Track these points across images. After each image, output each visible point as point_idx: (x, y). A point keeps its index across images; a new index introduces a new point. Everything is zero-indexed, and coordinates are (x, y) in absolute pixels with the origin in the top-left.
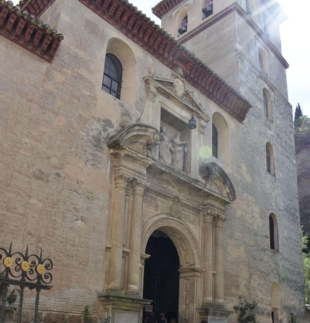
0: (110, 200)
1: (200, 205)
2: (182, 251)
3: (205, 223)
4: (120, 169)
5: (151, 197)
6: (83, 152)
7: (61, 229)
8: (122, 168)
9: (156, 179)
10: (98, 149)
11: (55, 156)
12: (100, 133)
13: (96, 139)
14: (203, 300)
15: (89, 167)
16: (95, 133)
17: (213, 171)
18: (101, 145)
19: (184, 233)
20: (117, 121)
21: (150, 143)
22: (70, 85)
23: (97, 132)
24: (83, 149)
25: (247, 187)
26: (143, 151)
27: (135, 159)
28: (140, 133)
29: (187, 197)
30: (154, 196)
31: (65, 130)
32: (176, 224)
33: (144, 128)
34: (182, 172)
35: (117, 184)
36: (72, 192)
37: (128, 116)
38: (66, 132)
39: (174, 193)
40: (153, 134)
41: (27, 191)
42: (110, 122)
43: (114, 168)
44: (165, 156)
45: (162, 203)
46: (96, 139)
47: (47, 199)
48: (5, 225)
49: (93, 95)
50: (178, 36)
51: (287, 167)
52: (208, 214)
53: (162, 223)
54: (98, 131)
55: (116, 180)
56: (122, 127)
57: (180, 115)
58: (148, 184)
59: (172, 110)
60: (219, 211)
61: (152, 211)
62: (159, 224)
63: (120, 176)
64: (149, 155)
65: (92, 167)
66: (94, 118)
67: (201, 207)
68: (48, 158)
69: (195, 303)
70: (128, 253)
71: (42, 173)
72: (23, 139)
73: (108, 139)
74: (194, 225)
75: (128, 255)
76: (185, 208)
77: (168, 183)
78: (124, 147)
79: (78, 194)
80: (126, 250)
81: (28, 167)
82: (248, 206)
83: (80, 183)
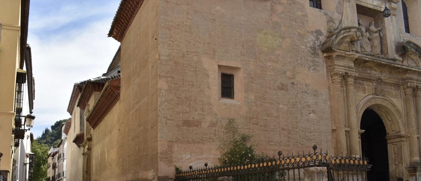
0: (330, 93)
1: (400, 80)
2: (388, 122)
3: (405, 95)
4: (334, 68)
5: (359, 83)
6: (306, 62)
7: (301, 122)
8: (336, 67)
9: (361, 67)
10: (315, 56)
11: (288, 70)
12: (315, 43)
13: (312, 49)
14: (411, 160)
15: (311, 72)
16: (311, 44)
17: (408, 49)
18: (317, 52)
19: (389, 107)
20: (325, 28)
21: (354, 40)
22: (288, 12)
23: (313, 43)
24: (305, 59)
26: (349, 48)
27: (344, 57)
28: (345, 35)
29: (388, 76)
30: (361, 82)
31: (291, 48)
32: (382, 101)
33: (348, 30)
34: (381, 56)
35: (333, 80)
36: (304, 94)
37: (332, 21)
38: (292, 49)
39: (377, 76)
40: (355, 33)
41: (276, 100)
42: (320, 31)
44: (367, 48)
45: (369, 86)
46: (312, 49)
47: (289, 102)
48: (268, 126)
49: (305, 14)
52: (408, 87)
53: (369, 103)
54: (313, 42)
55: (332, 77)
56: (330, 32)
57: (373, 5)
58: (357, 75)
59: (366, 3)
61: (362, 94)
62: (368, 104)
63: (336, 74)
64: (353, 49)
65: (313, 71)
66: (308, 32)
67: (401, 82)
68: (285, 72)
69: (404, 163)
70: (348, 131)
71: (283, 85)
72: (267, 64)
73: (321, 46)
74: (396, 98)
75: (348, 133)
76: (387, 86)
77: (371, 68)
78: (335, 50)
79: (308, 94)
80: (347, 129)
81: (274, 83)
83: (308, 86)
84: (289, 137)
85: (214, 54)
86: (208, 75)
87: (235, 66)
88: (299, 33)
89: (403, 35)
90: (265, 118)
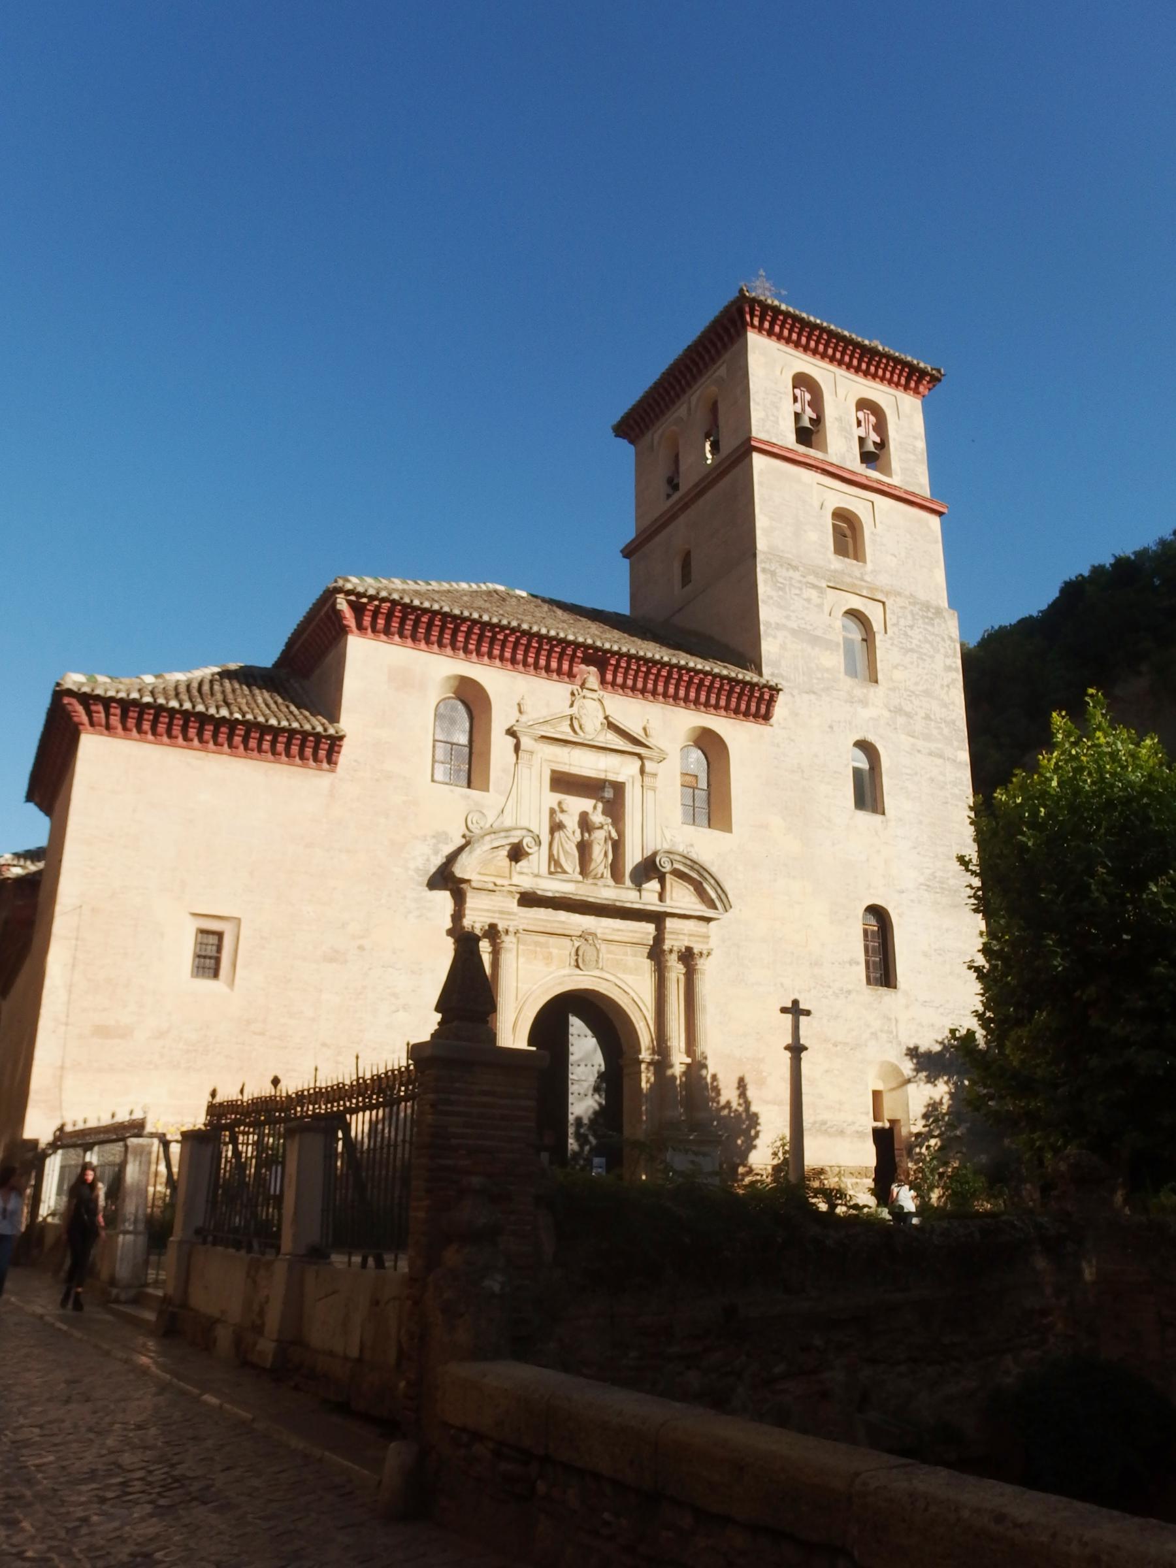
12: (428, 860)
30: (542, 939)
33: (503, 834)
42: (446, 833)
50: (669, 496)
51: (932, 780)
60: (692, 938)
84: (337, 1062)
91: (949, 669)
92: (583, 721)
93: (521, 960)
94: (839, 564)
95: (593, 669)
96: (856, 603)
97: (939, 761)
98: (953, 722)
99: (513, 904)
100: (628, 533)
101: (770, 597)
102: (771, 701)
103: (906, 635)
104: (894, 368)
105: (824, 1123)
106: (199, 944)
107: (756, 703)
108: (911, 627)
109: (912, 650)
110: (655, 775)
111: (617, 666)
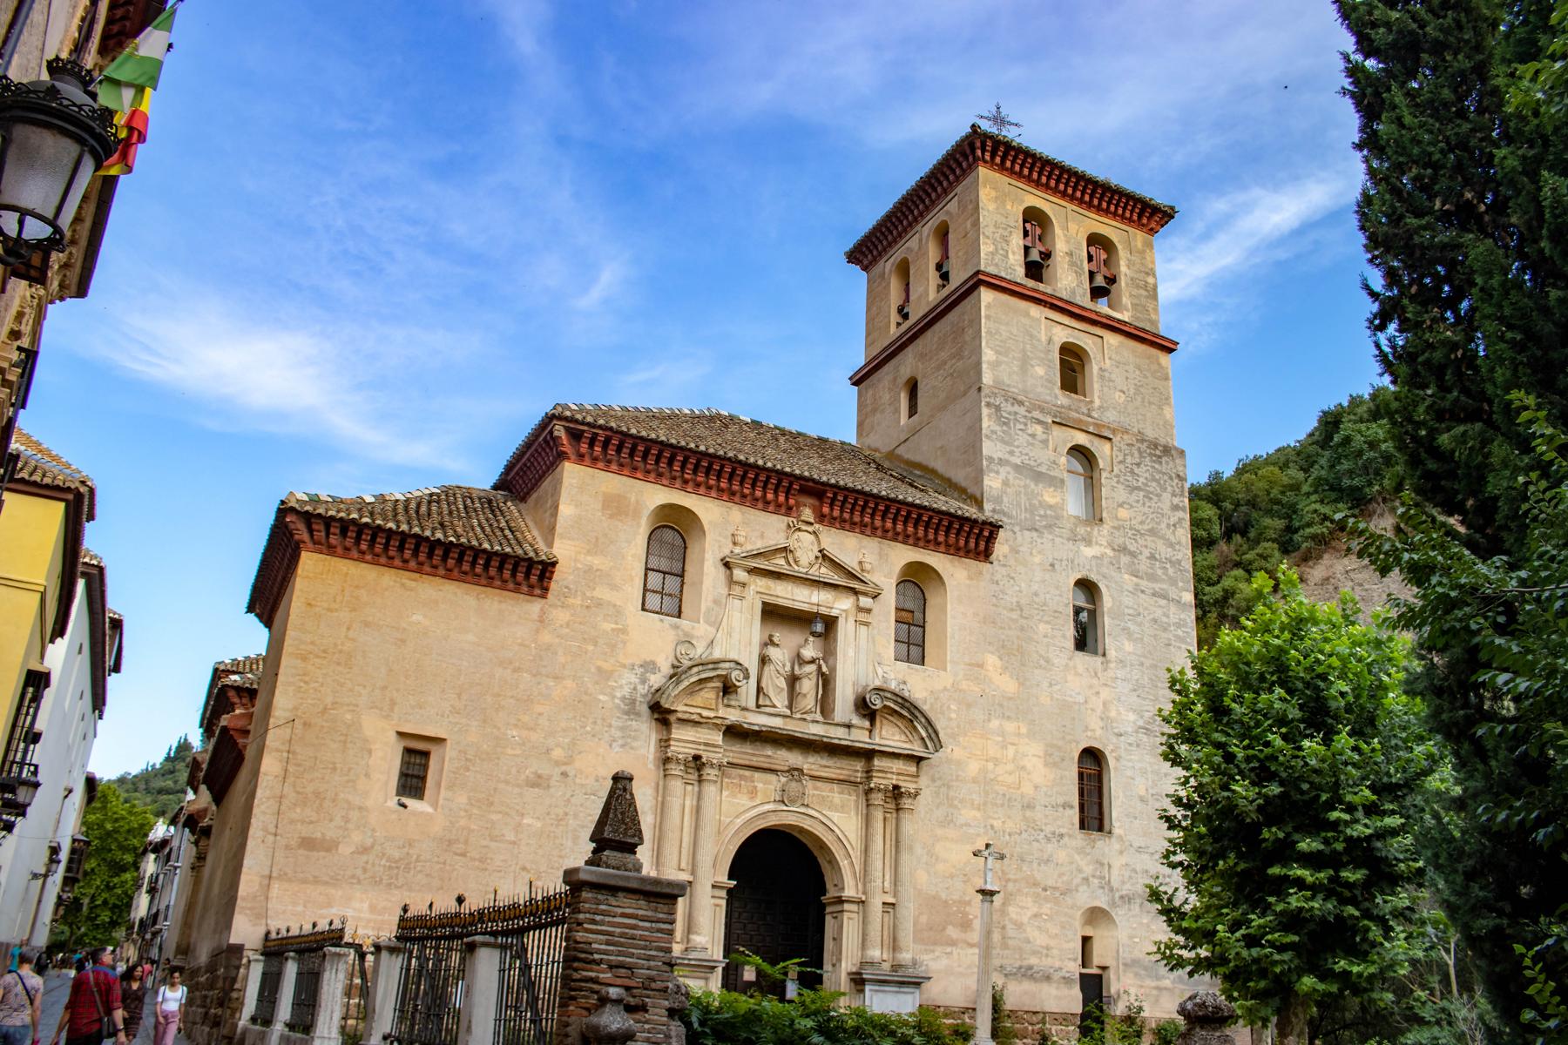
11: (558, 745)
16: (626, 691)
25: (1001, 705)
28: (704, 676)
30: (747, 773)
42: (654, 663)
43: (664, 743)
51: (1155, 621)
66: (624, 666)
68: (548, 751)
71: (540, 777)
82: (1004, 747)
85: (392, 710)
86: (370, 752)
87: (433, 735)
88: (599, 669)
89: (886, 669)
90: (484, 843)
91: (1176, 508)
92: (798, 554)
93: (725, 793)
94: (1063, 399)
95: (810, 501)
96: (1081, 439)
97: (1163, 602)
98: (1179, 562)
99: (718, 738)
100: (858, 359)
101: (994, 432)
102: (991, 539)
103: (1132, 472)
104: (1126, 204)
105: (1031, 968)
106: (405, 763)
107: (975, 538)
108: (1138, 465)
109: (1138, 488)
110: (869, 611)
111: (834, 500)
